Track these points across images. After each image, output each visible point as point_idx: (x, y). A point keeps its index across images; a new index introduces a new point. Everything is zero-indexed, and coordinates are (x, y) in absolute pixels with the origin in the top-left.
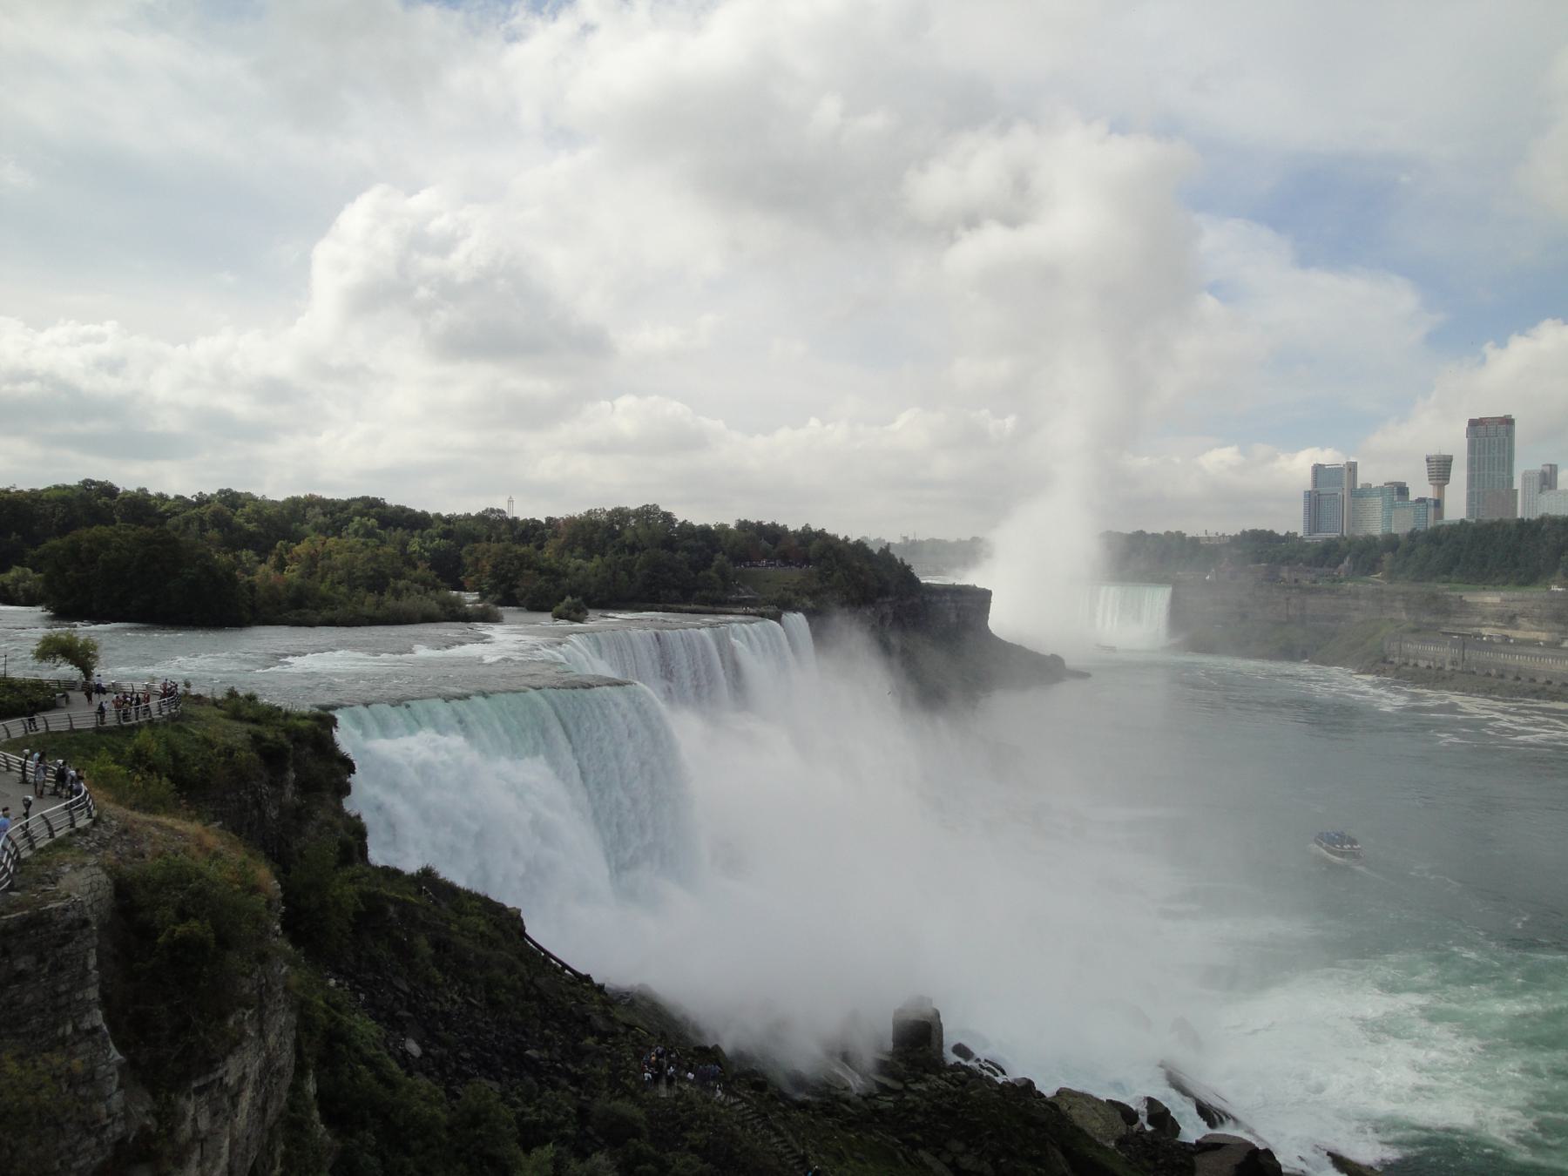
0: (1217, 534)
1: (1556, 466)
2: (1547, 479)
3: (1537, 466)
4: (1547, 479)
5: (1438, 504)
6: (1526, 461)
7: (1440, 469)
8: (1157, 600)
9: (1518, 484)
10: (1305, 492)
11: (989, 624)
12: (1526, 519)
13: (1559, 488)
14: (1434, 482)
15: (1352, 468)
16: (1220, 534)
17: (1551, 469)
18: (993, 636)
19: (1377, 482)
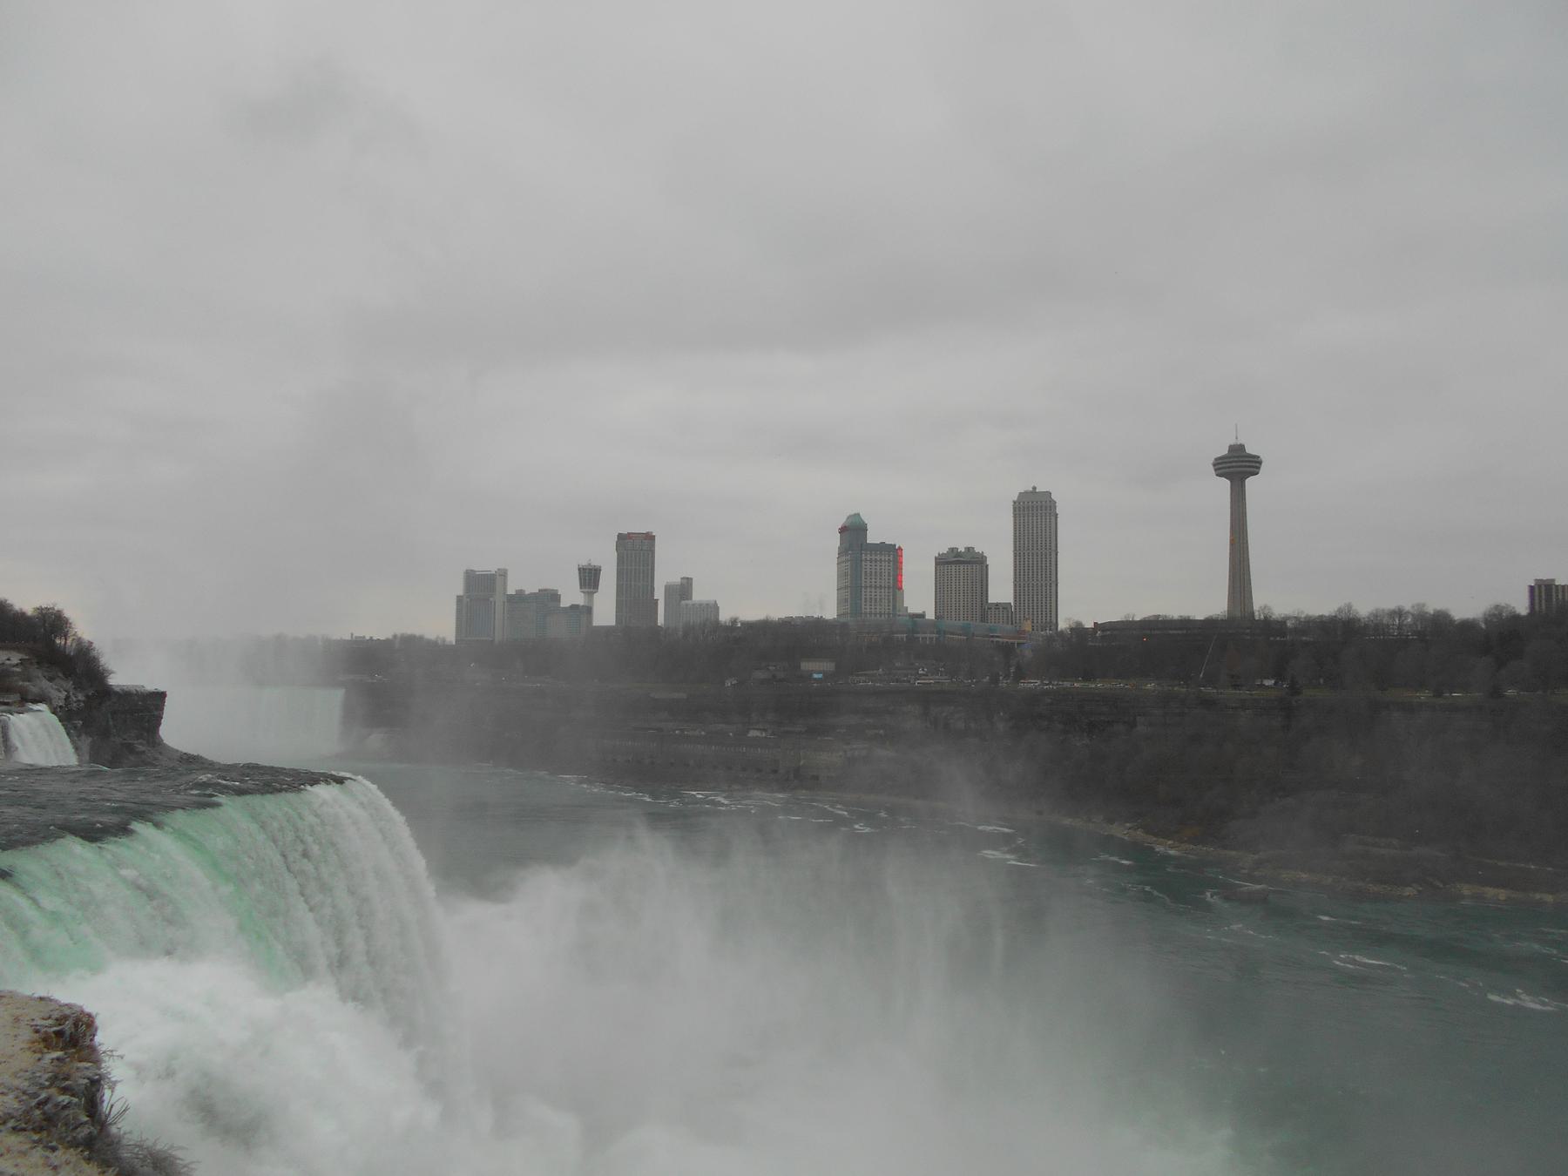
0: (364, 637)
1: (691, 579)
2: (683, 590)
3: (676, 580)
4: (683, 590)
5: (588, 610)
6: (665, 575)
7: (590, 577)
8: (334, 699)
9: (659, 594)
10: (458, 597)
11: (161, 733)
12: (691, 623)
13: (693, 599)
14: (586, 590)
15: (503, 574)
16: (368, 638)
17: (688, 583)
18: (165, 744)
19: (531, 588)
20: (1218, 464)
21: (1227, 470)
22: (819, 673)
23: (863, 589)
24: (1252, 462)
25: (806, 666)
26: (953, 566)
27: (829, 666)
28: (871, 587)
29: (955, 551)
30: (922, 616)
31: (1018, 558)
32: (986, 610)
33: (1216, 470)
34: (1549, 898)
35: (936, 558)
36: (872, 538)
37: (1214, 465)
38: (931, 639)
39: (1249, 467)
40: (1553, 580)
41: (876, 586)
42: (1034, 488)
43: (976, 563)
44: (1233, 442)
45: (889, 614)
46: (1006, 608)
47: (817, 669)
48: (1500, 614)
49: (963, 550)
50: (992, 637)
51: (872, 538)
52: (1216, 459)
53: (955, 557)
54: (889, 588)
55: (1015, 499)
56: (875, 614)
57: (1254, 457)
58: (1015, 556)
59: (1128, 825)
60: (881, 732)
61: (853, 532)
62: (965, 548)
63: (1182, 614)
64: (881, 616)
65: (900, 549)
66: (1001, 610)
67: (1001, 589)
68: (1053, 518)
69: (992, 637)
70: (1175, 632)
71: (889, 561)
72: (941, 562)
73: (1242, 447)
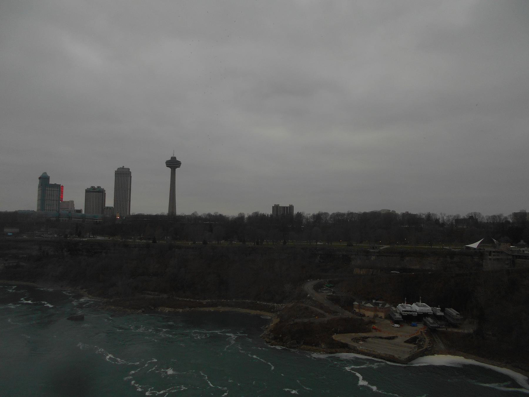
20: (167, 163)
21: (169, 165)
22: (10, 233)
23: (46, 201)
24: (178, 163)
25: (6, 230)
26: (92, 193)
27: (16, 230)
28: (49, 200)
29: (93, 187)
30: (79, 211)
31: (116, 191)
32: (103, 208)
33: (167, 165)
34: (181, 310)
35: (86, 190)
36: (52, 182)
37: (166, 163)
38: (65, 220)
39: (177, 165)
40: (279, 205)
41: (51, 200)
42: (123, 167)
43: (100, 192)
44: (172, 156)
45: (56, 210)
46: (111, 209)
47: (9, 231)
48: (258, 215)
49: (96, 187)
50: (94, 219)
51: (52, 182)
52: (166, 161)
53: (93, 190)
54: (57, 201)
55: (116, 170)
56: (51, 210)
57: (178, 161)
58: (115, 190)
59: (85, 290)
60: (25, 256)
61: (44, 180)
62: (97, 187)
63: (147, 214)
64: (53, 211)
65: (63, 186)
66: (109, 209)
67: (110, 202)
68: (129, 178)
69: (94, 219)
70: (145, 219)
71: (57, 191)
72: (88, 191)
73: (175, 158)
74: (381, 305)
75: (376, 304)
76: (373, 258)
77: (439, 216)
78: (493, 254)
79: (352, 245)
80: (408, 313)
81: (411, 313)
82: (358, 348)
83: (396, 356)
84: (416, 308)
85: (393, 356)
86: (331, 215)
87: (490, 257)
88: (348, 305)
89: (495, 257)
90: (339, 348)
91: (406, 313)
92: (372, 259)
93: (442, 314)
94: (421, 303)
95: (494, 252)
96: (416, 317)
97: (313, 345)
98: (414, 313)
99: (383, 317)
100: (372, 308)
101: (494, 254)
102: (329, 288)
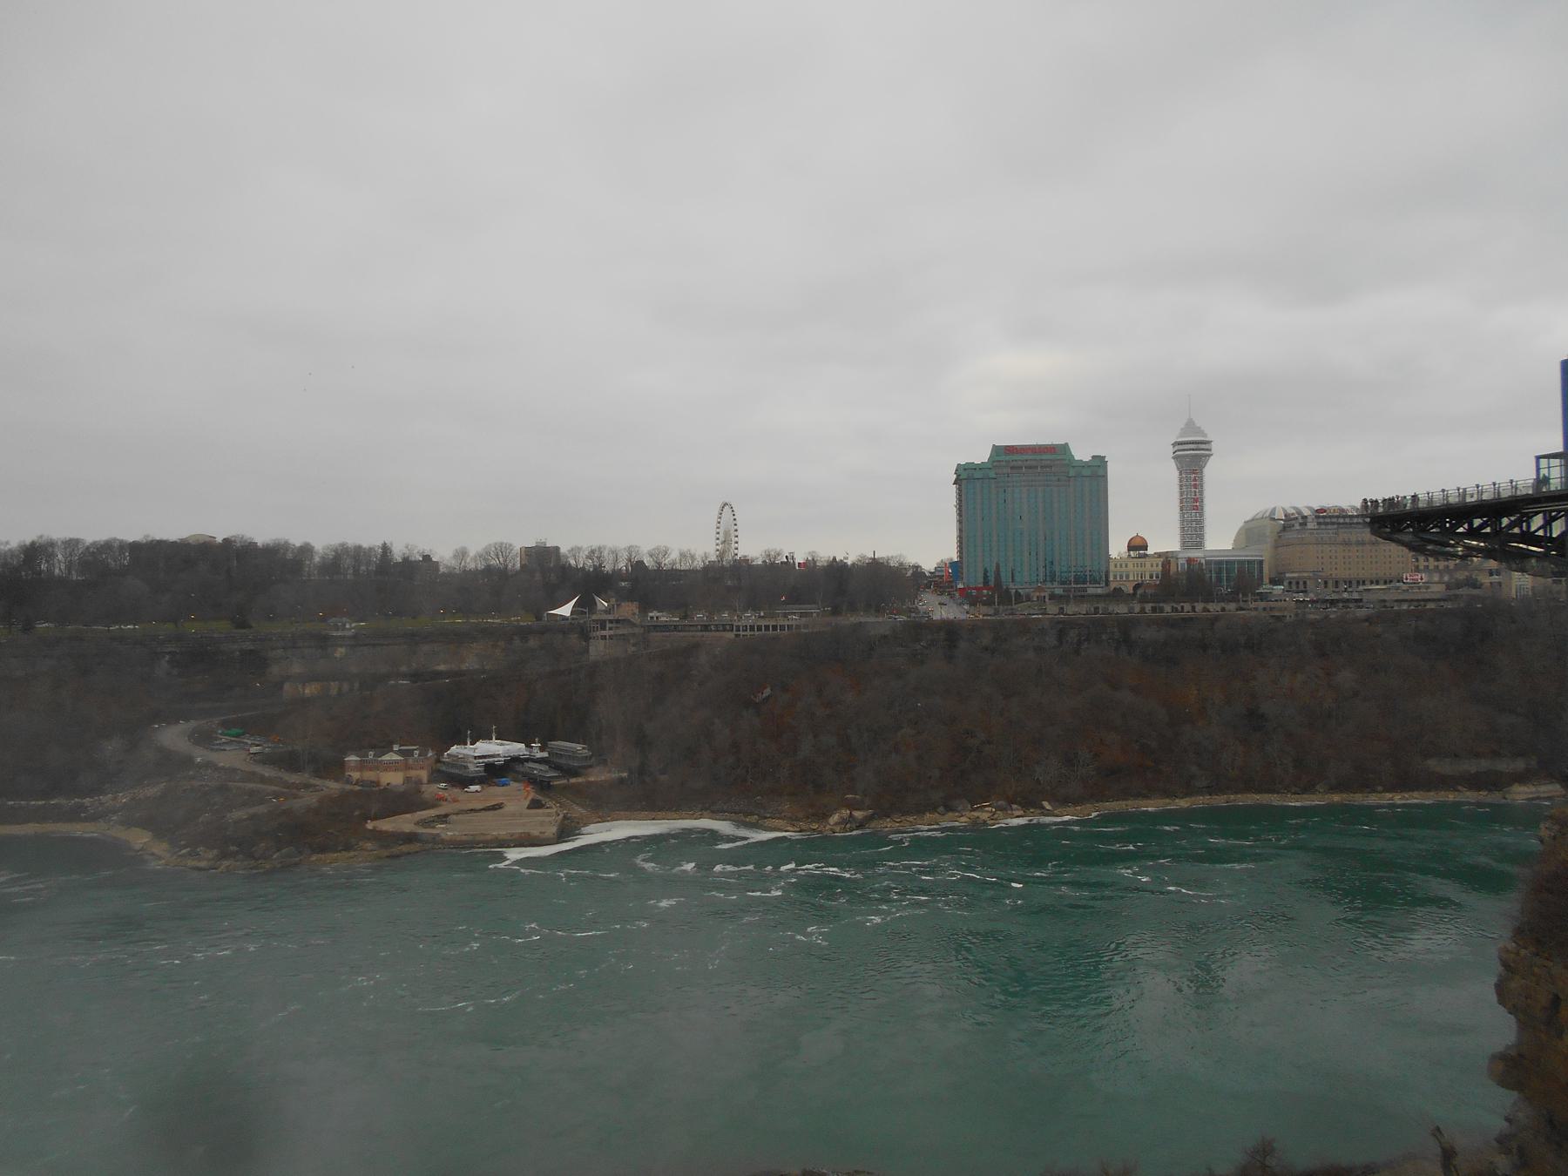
74: (417, 752)
75: (410, 753)
76: (340, 652)
77: (443, 554)
78: (608, 625)
79: (251, 627)
80: (486, 760)
81: (491, 760)
82: (443, 836)
83: (535, 832)
84: (496, 748)
85: (529, 834)
86: (88, 548)
87: (603, 633)
88: (333, 768)
89: (612, 632)
90: (401, 845)
91: (481, 761)
92: (337, 655)
93: (545, 754)
94: (471, 744)
95: (611, 621)
96: (501, 766)
97: (340, 848)
98: (496, 759)
99: (425, 780)
100: (396, 762)
101: (611, 625)
102: (233, 739)
